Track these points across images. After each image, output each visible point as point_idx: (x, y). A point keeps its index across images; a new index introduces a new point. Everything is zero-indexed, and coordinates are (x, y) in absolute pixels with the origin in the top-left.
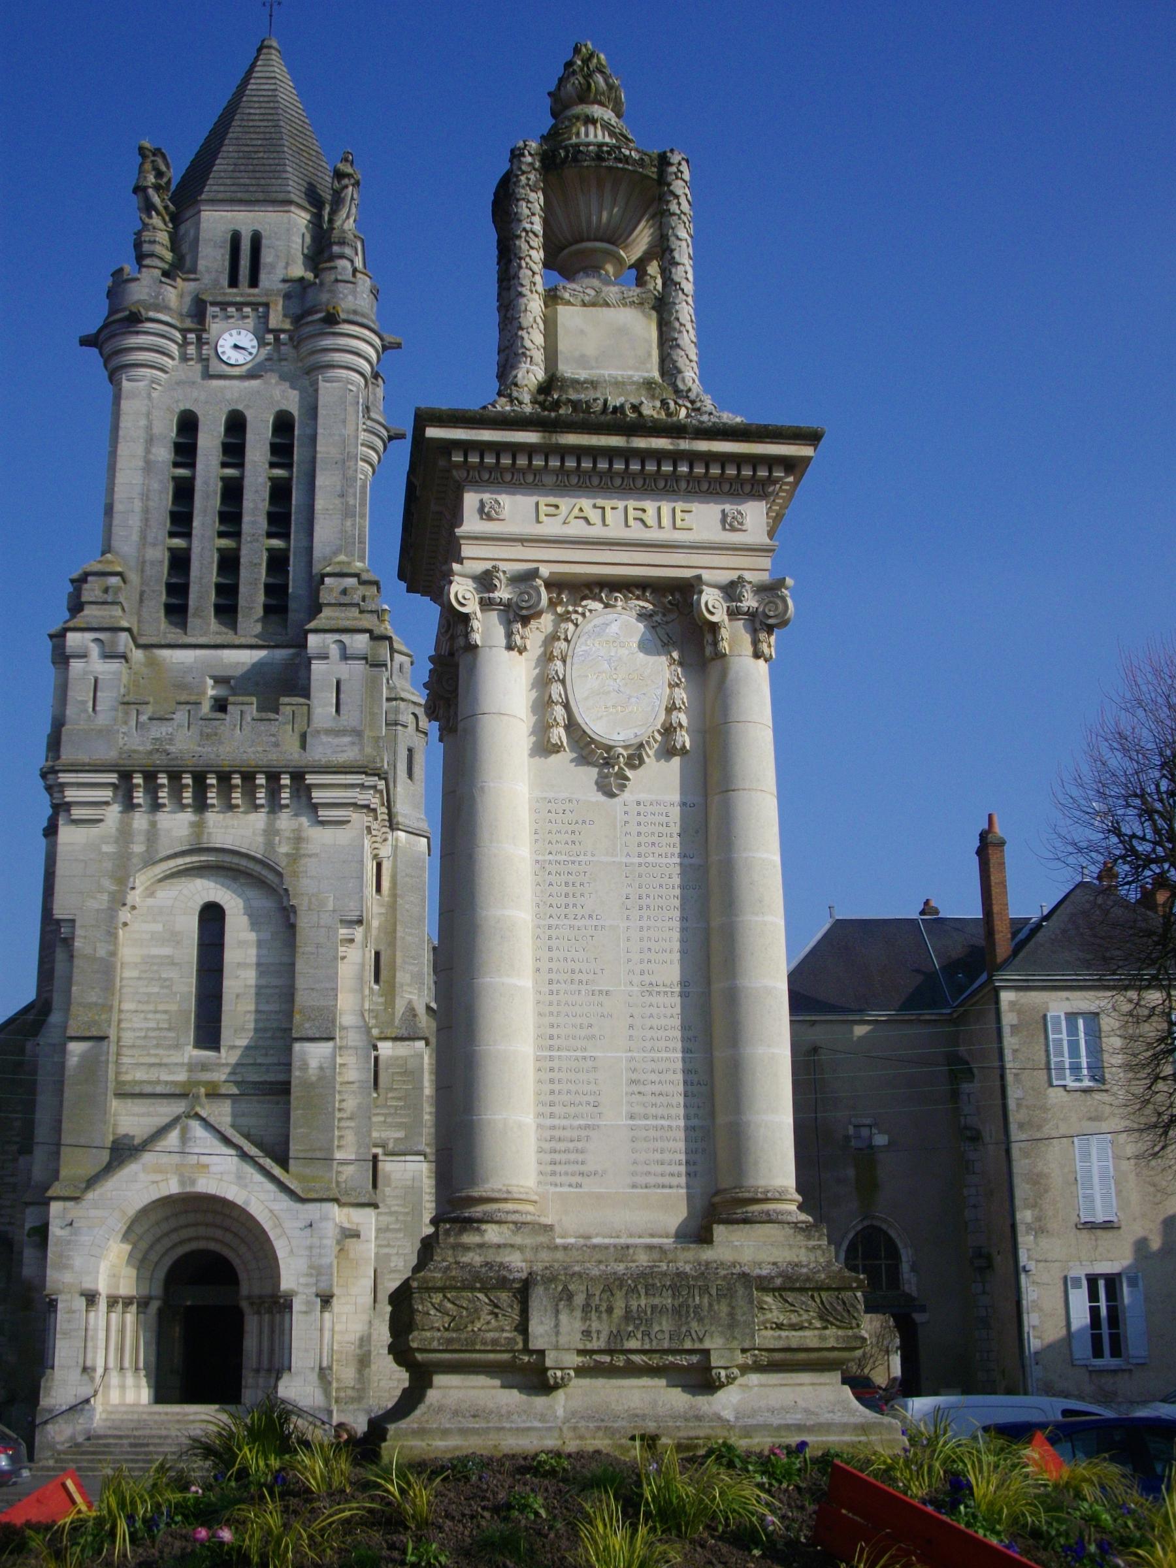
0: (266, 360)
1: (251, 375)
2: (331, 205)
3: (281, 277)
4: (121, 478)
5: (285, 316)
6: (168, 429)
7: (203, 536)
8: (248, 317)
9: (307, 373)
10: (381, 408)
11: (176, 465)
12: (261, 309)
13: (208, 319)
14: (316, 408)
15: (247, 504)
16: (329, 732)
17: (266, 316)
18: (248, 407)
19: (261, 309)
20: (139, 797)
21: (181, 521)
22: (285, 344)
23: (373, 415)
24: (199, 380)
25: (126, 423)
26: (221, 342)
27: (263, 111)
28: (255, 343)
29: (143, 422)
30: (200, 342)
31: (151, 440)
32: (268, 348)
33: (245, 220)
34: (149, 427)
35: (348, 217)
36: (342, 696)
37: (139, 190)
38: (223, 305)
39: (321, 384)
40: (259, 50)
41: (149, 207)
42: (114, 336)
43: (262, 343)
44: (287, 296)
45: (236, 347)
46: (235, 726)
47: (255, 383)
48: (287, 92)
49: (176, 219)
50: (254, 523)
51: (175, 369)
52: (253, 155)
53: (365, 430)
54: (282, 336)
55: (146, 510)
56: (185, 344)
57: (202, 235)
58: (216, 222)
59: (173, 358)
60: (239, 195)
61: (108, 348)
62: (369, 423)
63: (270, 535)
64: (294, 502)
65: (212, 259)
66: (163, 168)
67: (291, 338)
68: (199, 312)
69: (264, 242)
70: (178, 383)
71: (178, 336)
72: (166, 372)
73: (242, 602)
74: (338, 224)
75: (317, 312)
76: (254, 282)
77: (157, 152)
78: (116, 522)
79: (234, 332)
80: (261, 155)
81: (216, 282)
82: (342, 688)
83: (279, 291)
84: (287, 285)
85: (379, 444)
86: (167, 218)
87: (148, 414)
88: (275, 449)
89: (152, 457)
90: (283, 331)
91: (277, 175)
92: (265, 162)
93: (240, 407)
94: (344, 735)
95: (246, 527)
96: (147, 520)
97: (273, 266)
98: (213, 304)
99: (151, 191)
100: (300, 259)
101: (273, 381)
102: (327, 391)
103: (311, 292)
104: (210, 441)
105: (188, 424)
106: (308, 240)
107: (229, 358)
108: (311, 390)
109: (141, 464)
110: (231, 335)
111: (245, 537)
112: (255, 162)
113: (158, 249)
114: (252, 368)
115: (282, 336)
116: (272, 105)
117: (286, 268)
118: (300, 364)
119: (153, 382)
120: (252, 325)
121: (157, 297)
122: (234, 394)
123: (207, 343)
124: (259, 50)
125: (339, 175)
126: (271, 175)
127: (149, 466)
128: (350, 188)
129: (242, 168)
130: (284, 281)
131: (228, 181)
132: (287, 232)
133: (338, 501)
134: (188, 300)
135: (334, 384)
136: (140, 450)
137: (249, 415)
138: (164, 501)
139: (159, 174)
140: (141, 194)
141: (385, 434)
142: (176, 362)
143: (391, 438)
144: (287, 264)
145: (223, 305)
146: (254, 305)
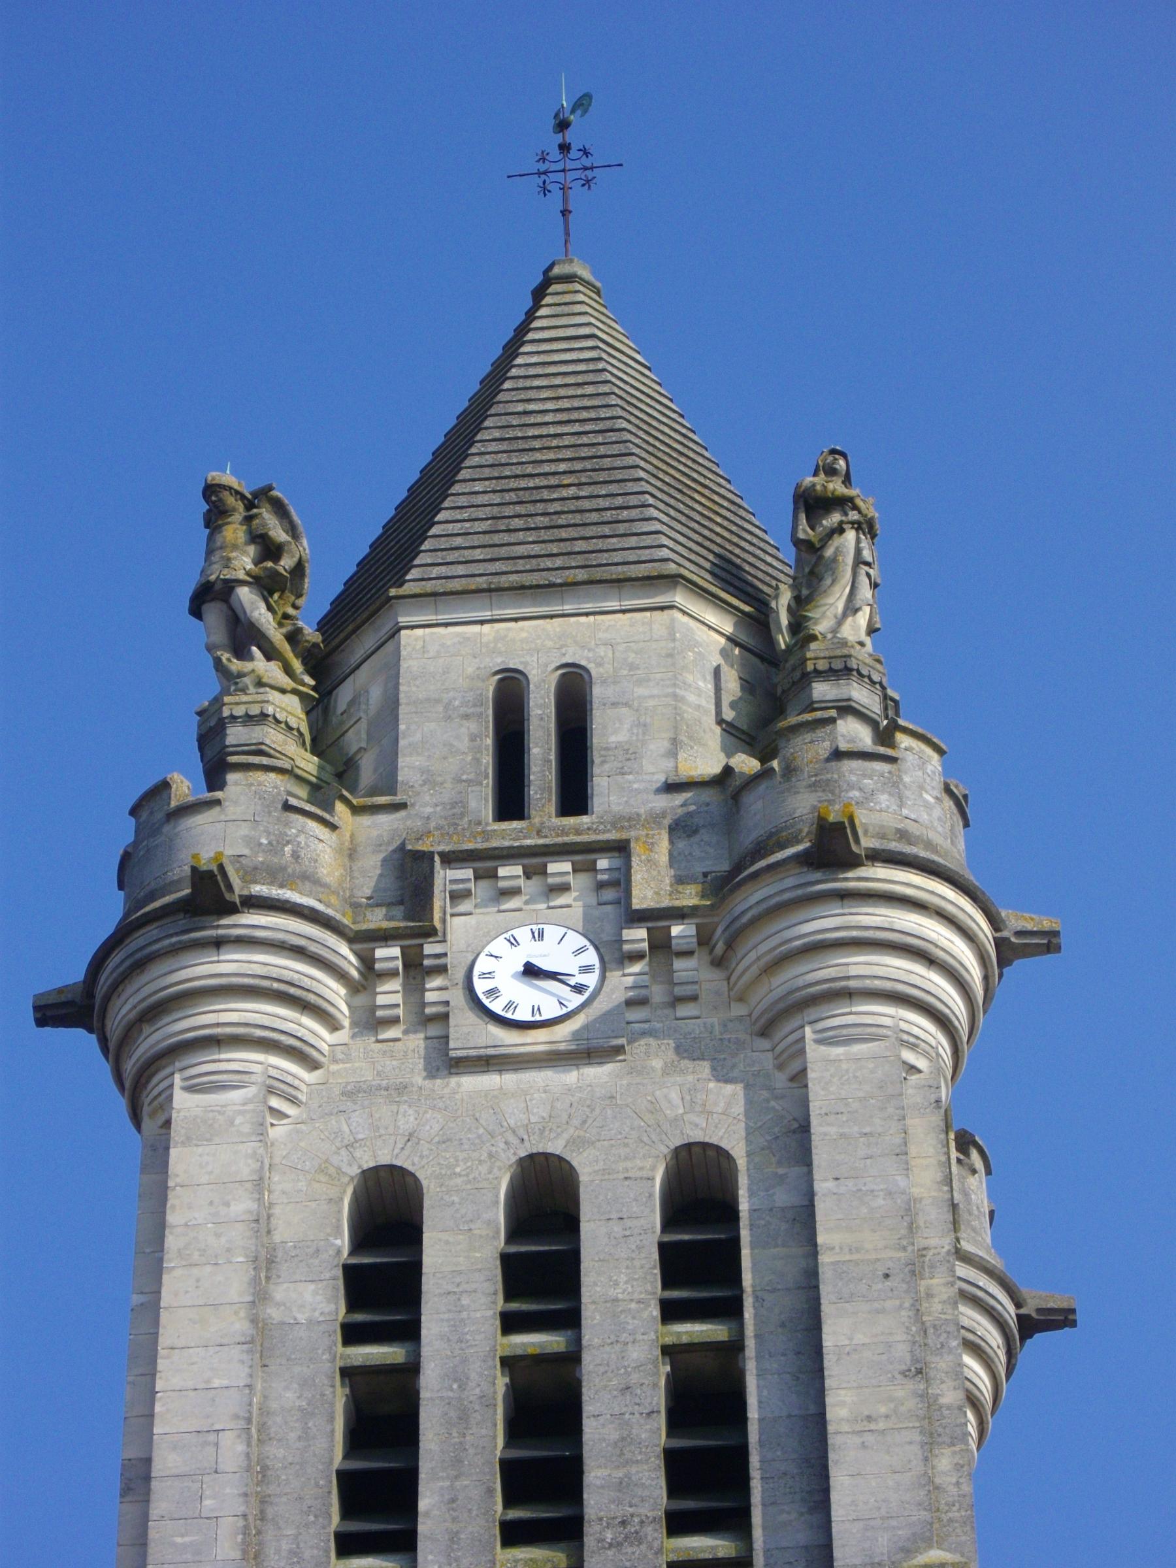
0: (629, 1003)
1: (588, 1051)
2: (795, 587)
3: (661, 778)
4: (173, 1375)
5: (680, 880)
6: (322, 1232)
7: (454, 1537)
8: (564, 888)
9: (764, 1033)
10: (989, 1240)
11: (352, 1334)
12: (603, 863)
13: (439, 901)
14: (804, 1129)
15: (597, 1431)
17: (622, 882)
18: (578, 1143)
19: (603, 863)
22: (689, 953)
24: (419, 1079)
25: (185, 1212)
28: (591, 957)
29: (243, 1205)
30: (416, 969)
31: (271, 1262)
32: (637, 968)
33: (538, 642)
34: (261, 1223)
35: (851, 609)
37: (209, 595)
38: (485, 861)
39: (814, 1052)
40: (539, 294)
41: (243, 636)
42: (140, 965)
43: (613, 956)
44: (680, 828)
45: (531, 971)
47: (597, 1074)
48: (628, 366)
49: (324, 666)
50: (622, 1486)
51: (340, 1053)
54: (676, 930)
55: (259, 1472)
56: (371, 972)
57: (405, 690)
58: (445, 660)
59: (334, 1027)
61: (123, 1009)
62: (963, 1270)
63: (677, 1524)
64: (753, 1413)
65: (440, 757)
66: (279, 534)
67: (704, 939)
68: (411, 881)
69: (598, 692)
70: (351, 1094)
71: (345, 954)
72: (313, 1065)
74: (821, 627)
75: (782, 846)
76: (574, 795)
77: (263, 494)
78: (158, 1507)
79: (523, 934)
81: (458, 805)
83: (655, 818)
84: (679, 799)
85: (994, 1339)
86: (297, 665)
87: (259, 1184)
88: (676, 1264)
89: (273, 1313)
90: (679, 914)
91: (622, 528)
93: (555, 1147)
95: (597, 1499)
96: (264, 1501)
97: (631, 754)
98: (451, 859)
99: (246, 595)
100: (714, 736)
101: (657, 1064)
102: (837, 1070)
103: (755, 805)
104: (461, 1259)
105: (388, 1219)
106: (732, 685)
107: (510, 1005)
108: (781, 1080)
109: (240, 1326)
110: (513, 942)
112: (557, 507)
113: (272, 737)
114: (586, 1027)
115: (676, 930)
117: (673, 753)
118: (739, 1010)
119: (271, 1091)
120: (578, 910)
121: (275, 848)
122: (533, 1109)
123: (442, 970)
124: (539, 294)
126: (606, 530)
127: (263, 1341)
128: (850, 535)
130: (671, 787)
132: (664, 676)
133: (904, 1391)
134: (370, 872)
135: (857, 1048)
136: (234, 1285)
138: (316, 1442)
139: (270, 550)
140: (214, 612)
141: (1009, 1310)
142: (343, 1036)
144: (675, 742)
145: (485, 861)
146: (582, 853)
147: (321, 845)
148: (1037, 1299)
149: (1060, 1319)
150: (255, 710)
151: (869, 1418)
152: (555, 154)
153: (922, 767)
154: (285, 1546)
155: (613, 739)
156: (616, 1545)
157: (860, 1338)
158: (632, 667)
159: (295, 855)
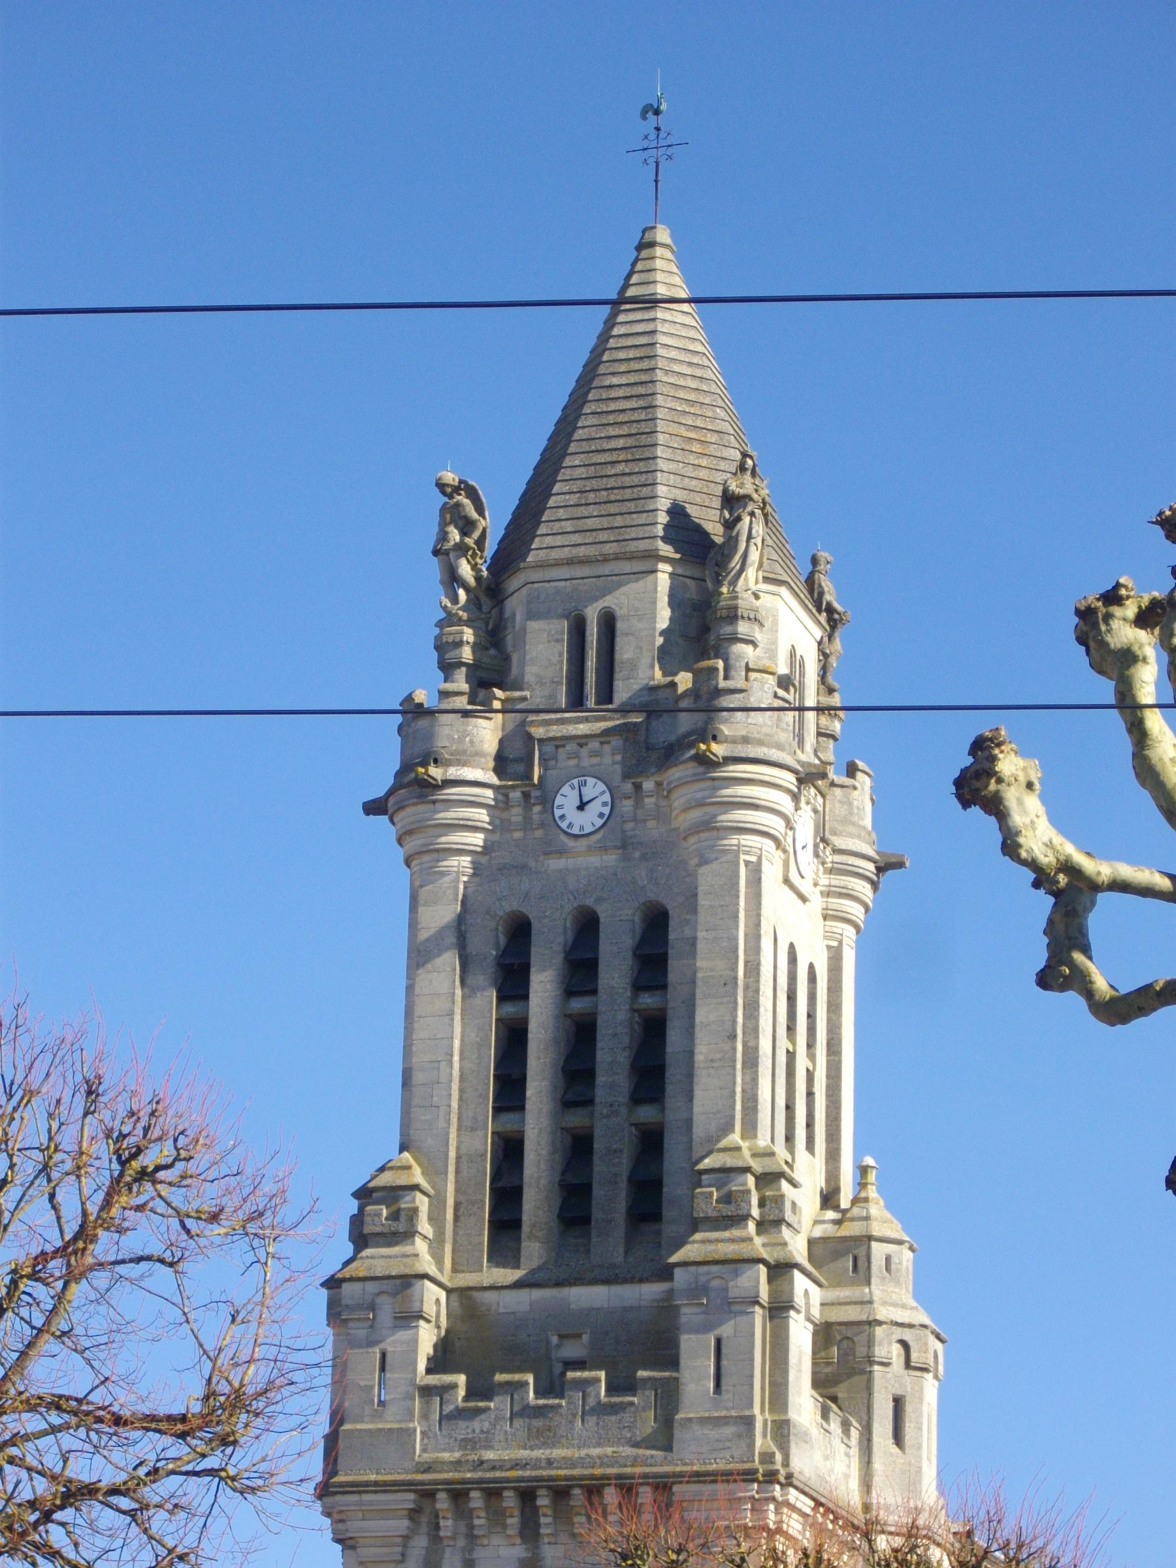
10: (868, 822)
15: (602, 1056)
16: (703, 1421)
20: (447, 1525)
21: (510, 1090)
23: (840, 842)
26: (559, 800)
27: (632, 378)
36: (724, 1363)
46: (575, 1416)
52: (611, 471)
53: (831, 871)
60: (582, 551)
69: (620, 625)
70: (503, 868)
73: (597, 1213)
80: (620, 468)
82: (724, 1351)
92: (627, 481)
93: (589, 902)
94: (726, 1424)
97: (633, 665)
111: (600, 1109)
116: (645, 365)
125: (731, 501)
126: (631, 506)
129: (591, 497)
131: (568, 526)
137: (604, 913)
143: (880, 870)
147: (485, 732)
148: (894, 850)
149: (900, 865)
150: (457, 640)
151: (712, 1061)
152: (653, 136)
153: (762, 689)
154: (471, 1114)
155: (626, 656)
156: (608, 1116)
157: (712, 1018)
158: (637, 610)
159: (472, 742)
